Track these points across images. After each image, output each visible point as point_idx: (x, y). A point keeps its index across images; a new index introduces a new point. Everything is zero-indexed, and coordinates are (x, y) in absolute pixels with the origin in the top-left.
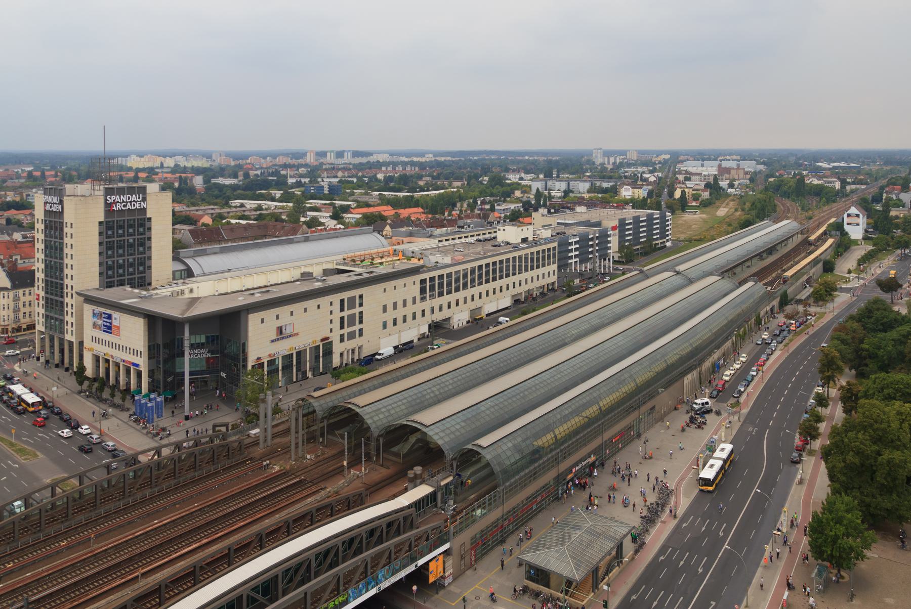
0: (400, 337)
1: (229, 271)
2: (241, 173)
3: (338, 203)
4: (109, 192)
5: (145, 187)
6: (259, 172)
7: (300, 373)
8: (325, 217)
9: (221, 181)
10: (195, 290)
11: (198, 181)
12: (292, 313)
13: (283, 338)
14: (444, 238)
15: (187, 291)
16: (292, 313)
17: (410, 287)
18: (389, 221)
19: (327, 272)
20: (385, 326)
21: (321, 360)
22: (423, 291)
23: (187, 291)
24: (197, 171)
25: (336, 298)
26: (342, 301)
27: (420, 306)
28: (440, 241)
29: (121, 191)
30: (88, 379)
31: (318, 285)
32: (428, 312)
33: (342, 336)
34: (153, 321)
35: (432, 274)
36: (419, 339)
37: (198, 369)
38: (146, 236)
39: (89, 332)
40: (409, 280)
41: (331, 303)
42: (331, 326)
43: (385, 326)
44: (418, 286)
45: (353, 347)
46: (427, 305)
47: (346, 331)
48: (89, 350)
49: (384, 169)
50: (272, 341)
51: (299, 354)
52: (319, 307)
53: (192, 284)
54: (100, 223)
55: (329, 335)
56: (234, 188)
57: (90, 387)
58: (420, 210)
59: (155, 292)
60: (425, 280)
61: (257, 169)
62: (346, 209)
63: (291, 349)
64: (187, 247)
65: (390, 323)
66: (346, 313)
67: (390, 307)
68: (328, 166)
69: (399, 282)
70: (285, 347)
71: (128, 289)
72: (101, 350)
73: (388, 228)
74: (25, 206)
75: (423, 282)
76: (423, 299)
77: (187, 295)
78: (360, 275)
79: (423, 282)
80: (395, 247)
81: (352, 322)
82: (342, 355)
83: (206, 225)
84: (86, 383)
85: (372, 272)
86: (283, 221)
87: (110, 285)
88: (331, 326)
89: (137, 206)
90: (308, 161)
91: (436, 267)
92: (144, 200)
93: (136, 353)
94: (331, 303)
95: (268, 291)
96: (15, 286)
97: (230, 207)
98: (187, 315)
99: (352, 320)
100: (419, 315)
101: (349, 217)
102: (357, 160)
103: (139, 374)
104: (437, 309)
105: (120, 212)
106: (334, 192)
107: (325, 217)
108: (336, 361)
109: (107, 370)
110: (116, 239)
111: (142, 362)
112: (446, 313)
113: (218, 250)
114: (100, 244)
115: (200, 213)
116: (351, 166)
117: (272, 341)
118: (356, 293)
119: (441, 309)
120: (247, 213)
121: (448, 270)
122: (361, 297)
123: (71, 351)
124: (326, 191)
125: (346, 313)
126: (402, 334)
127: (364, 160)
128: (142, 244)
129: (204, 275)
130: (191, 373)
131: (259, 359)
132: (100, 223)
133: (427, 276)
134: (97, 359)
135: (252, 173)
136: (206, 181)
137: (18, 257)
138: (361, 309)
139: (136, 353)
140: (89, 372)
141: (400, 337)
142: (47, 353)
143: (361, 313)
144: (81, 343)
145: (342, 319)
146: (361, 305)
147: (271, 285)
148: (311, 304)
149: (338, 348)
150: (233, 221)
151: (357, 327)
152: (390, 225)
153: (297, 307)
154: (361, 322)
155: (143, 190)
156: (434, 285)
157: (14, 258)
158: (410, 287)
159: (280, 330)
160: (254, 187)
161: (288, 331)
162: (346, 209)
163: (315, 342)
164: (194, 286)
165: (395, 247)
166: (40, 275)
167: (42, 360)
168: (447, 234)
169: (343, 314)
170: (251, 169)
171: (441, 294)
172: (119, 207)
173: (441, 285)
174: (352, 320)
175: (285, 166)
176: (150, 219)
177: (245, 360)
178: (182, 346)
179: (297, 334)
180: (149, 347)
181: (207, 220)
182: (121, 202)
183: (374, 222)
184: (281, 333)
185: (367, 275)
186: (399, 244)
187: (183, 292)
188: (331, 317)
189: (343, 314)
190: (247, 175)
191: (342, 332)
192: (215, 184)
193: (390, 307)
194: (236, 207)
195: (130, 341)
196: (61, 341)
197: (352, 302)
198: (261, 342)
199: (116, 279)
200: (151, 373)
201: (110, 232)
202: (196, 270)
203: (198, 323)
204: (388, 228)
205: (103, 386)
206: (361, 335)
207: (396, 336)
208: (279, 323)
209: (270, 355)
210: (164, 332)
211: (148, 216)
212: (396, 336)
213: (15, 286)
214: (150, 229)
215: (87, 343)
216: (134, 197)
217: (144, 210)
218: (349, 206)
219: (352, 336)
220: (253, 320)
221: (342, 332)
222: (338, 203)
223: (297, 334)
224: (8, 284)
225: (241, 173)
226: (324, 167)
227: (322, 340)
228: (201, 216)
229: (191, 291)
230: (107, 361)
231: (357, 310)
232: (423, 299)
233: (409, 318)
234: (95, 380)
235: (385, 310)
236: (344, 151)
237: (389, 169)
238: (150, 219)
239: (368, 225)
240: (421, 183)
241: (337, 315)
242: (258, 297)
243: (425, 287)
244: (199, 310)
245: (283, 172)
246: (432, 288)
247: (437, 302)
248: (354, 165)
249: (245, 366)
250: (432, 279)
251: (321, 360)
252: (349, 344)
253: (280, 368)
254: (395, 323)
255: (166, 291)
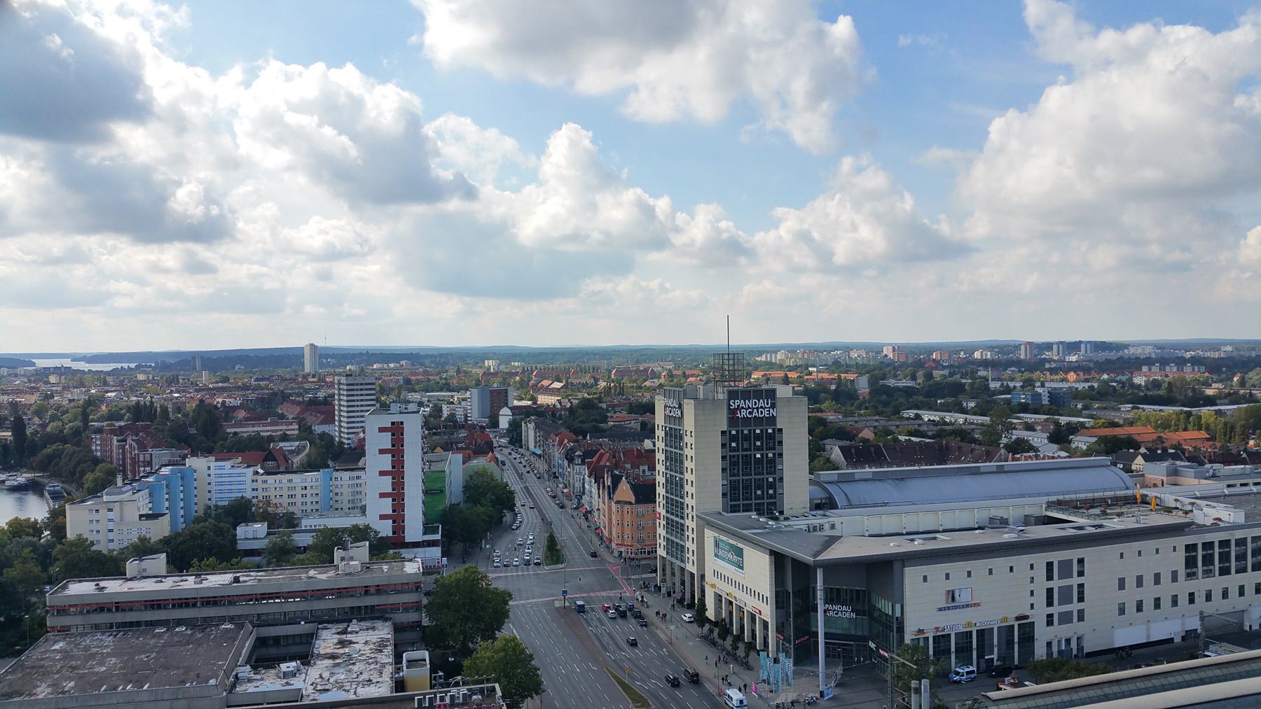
0: (1148, 630)
1: (886, 504)
2: (920, 374)
3: (1064, 420)
4: (733, 395)
5: (774, 391)
6: (946, 372)
7: (982, 661)
8: (1038, 439)
9: (892, 382)
10: (838, 526)
11: (863, 386)
12: (969, 574)
13: (956, 608)
14: (1238, 482)
15: (827, 526)
16: (969, 574)
17: (1171, 554)
18: (1143, 450)
19: (1028, 521)
20: (1122, 611)
21: (1016, 647)
22: (1190, 562)
23: (827, 526)
24: (861, 369)
25: (1040, 559)
26: (1050, 565)
27: (1184, 587)
28: (1229, 486)
29: (746, 394)
30: (709, 620)
31: (1007, 537)
32: (1200, 599)
33: (1050, 616)
34: (779, 560)
35: (1208, 537)
36: (1183, 638)
37: (839, 632)
38: (777, 452)
39: (713, 564)
40: (1165, 543)
41: (1032, 567)
42: (1032, 600)
43: (1122, 611)
44: (1181, 555)
45: (1068, 636)
46: (1200, 585)
47: (1056, 609)
48: (713, 586)
49: (1145, 369)
50: (940, 609)
51: (981, 633)
52: (991, 572)
53: (835, 517)
54: (723, 433)
55: (1028, 612)
56: (908, 392)
57: (711, 631)
58: (1204, 434)
59: (786, 523)
60: (1195, 545)
61: (944, 368)
62: (1074, 429)
63: (969, 624)
64: (837, 469)
65: (1131, 608)
66: (1075, 581)
67: (1131, 583)
68: (1053, 365)
69: (1149, 545)
70: (955, 622)
71: (754, 515)
72: (725, 588)
73: (1139, 460)
74: (650, 408)
75: (1190, 548)
76: (1191, 576)
77: (828, 532)
78: (1081, 528)
79: (1190, 548)
80: (1145, 491)
81: (1066, 597)
82: (1049, 644)
83: (865, 441)
84: (707, 626)
85: (1100, 526)
86: (975, 441)
87: (734, 509)
88: (1032, 600)
89: (766, 413)
90: (1022, 357)
91: (1216, 526)
92: (773, 406)
93: (760, 597)
94: (1032, 567)
95: (935, 538)
96: (638, 501)
97: (902, 418)
98: (826, 556)
99: (1066, 596)
100: (1183, 599)
101: (1081, 442)
102: (1102, 356)
103: (765, 624)
104: (1217, 595)
105: (746, 421)
106: (1058, 402)
107: (1038, 439)
108: (1040, 652)
109: (731, 613)
110: (740, 453)
111: (767, 612)
112: (1235, 602)
113: (835, 478)
114: (723, 458)
115: (860, 425)
116: (1092, 365)
117: (940, 609)
118: (1073, 554)
119: (1225, 594)
120: (922, 429)
121: (1239, 534)
122: (1081, 561)
123: (692, 585)
124: (1045, 401)
125: (1056, 584)
126: (1152, 625)
127: (1113, 355)
128: (772, 463)
129: (850, 505)
130: (827, 635)
131: (921, 631)
132: (723, 433)
133: (1198, 539)
134: (718, 598)
135: (937, 374)
136: (873, 382)
137: (646, 468)
138: (1081, 580)
139: (760, 597)
140: (710, 613)
141: (1148, 630)
142: (669, 584)
143: (1081, 586)
144: (703, 577)
145: (1050, 591)
146: (1081, 574)
147: (944, 531)
148: (1001, 563)
149: (1043, 634)
150: (902, 438)
151: (1075, 607)
152: (1144, 456)
153: (979, 566)
154: (1081, 599)
155: (771, 394)
156: (1212, 556)
157: (642, 468)
158: (1171, 554)
159: (952, 596)
160: (932, 394)
161: (963, 598)
162: (1074, 429)
163: (1005, 619)
164: (837, 520)
165: (1145, 491)
166: (660, 490)
167: (663, 590)
168: (1243, 475)
169: (1050, 584)
170: (936, 369)
171: (1225, 571)
172: (744, 413)
173: (1225, 557)
174: (1066, 596)
175: (985, 363)
176: (780, 430)
177: (901, 630)
178: (815, 598)
179: (978, 605)
180: (777, 593)
181: (867, 434)
182: (747, 407)
183: (1117, 448)
184: (953, 599)
185: (1093, 530)
186: (1155, 485)
187: (821, 528)
188: (1032, 587)
189: (1050, 584)
190: (929, 376)
191: (1050, 610)
192: (884, 386)
193: (1131, 583)
194: (908, 419)
195: (743, 580)
196: (683, 570)
197: (1066, 568)
198: (923, 607)
199: (741, 502)
200: (780, 629)
201: (734, 445)
202: (840, 500)
203: (835, 568)
204: (1139, 460)
205: (727, 635)
206: (1081, 617)
207: (1179, 621)
208: (950, 585)
209: (937, 628)
210: (793, 578)
211: (779, 427)
212: (1179, 621)
213: (638, 501)
214: (781, 443)
215: (709, 577)
216: (761, 403)
217: (772, 420)
218: (1082, 424)
219: (1066, 618)
220: (912, 575)
221: (1050, 610)
222: (1064, 420)
223: (978, 605)
224: (633, 500)
225: (920, 374)
226: (1047, 366)
227: (1018, 618)
228: (860, 430)
229: (833, 527)
230: (731, 603)
231: (1075, 581)
232: (1191, 576)
233: (1166, 603)
234: (716, 624)
235: (1122, 584)
236: (1081, 342)
237: (1154, 368)
238: (780, 430)
239: (1107, 453)
240: (1209, 392)
241: (1042, 585)
242: (918, 545)
243: (1195, 558)
244: (837, 552)
245: (982, 373)
246: (1208, 560)
247: (1217, 583)
248: (1096, 363)
249: (902, 639)
250: (1208, 546)
251: (1016, 647)
252: (1060, 632)
253: (953, 649)
254: (1140, 607)
255: (801, 524)
